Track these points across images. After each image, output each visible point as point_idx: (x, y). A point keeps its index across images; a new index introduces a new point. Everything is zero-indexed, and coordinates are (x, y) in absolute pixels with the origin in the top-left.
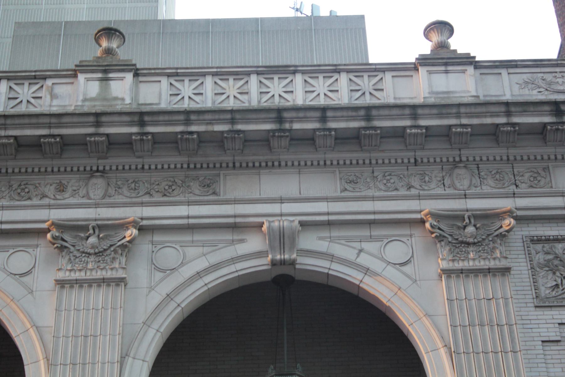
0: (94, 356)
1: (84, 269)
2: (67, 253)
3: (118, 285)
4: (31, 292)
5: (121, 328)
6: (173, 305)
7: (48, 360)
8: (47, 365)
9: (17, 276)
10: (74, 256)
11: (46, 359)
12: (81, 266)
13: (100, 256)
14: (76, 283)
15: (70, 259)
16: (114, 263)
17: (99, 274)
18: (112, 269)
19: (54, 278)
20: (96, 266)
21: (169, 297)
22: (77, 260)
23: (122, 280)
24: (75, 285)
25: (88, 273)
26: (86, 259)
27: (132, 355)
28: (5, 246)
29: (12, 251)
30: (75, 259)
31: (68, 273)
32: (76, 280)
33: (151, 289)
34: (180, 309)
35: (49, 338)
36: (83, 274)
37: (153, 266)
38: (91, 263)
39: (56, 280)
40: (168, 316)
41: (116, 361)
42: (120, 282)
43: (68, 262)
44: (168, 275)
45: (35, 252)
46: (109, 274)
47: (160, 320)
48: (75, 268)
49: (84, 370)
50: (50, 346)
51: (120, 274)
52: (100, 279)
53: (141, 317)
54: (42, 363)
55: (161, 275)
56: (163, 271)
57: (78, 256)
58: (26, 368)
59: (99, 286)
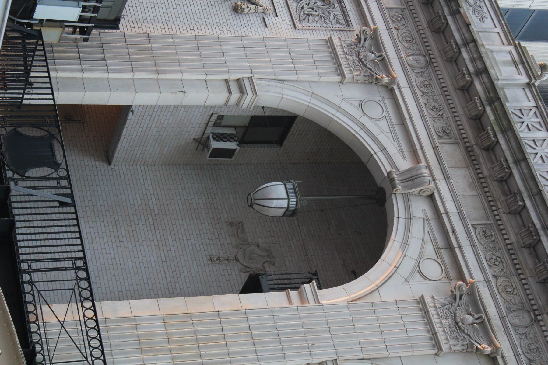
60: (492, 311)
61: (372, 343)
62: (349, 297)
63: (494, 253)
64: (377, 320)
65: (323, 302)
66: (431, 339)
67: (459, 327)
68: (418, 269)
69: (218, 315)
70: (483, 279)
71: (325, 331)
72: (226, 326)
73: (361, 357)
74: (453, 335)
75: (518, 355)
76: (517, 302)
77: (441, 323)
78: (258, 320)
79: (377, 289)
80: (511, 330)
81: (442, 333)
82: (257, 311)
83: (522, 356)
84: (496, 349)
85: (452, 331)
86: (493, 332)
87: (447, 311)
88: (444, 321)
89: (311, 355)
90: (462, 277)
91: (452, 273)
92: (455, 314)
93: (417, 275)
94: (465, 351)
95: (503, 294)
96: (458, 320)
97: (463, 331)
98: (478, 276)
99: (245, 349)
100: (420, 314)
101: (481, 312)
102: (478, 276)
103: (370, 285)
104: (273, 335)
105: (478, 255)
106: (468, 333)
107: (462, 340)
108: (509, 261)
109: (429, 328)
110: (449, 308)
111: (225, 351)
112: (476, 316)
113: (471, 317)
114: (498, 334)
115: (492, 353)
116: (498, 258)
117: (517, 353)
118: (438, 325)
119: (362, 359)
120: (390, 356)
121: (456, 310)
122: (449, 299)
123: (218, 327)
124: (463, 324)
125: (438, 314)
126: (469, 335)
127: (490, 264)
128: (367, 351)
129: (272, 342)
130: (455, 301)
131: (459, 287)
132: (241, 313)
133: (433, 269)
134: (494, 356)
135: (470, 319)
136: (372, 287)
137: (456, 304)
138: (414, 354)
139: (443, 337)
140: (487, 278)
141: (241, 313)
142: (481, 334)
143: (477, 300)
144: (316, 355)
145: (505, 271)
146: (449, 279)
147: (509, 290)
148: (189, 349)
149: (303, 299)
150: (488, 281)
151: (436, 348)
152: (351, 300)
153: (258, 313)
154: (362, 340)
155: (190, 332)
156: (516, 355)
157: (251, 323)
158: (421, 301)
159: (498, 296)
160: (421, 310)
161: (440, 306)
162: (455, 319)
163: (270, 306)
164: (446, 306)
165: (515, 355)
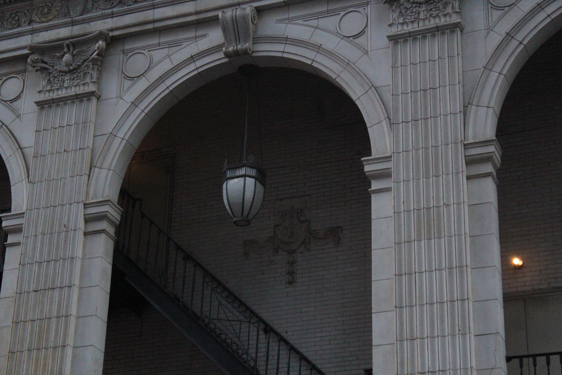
0: (435, 108)
1: (417, 20)
2: (396, 6)
3: (453, 32)
4: (367, 53)
5: (461, 77)
6: (514, 43)
7: (390, 119)
8: (389, 125)
9: (351, 38)
10: (405, 8)
11: (387, 119)
12: (413, 17)
13: (431, 3)
14: (410, 36)
15: (401, 12)
16: (447, 9)
17: (432, 23)
18: (445, 15)
19: (387, 35)
20: (428, 15)
21: (509, 36)
22: (409, 11)
23: (457, 25)
24: (409, 39)
25: (421, 24)
26: (417, 9)
27: (475, 103)
28: (336, 9)
29: (343, 13)
30: (406, 12)
31: (400, 27)
32: (409, 33)
33: (489, 29)
34: (523, 46)
35: (388, 97)
36: (416, 25)
37: (490, 5)
38: (423, 13)
39: (388, 37)
40: (510, 56)
41: (459, 111)
42: (454, 27)
43: (399, 15)
44: (506, 14)
45: (366, 11)
46: (442, 21)
47: (501, 61)
48: (407, 21)
49: (426, 126)
50: (390, 105)
51: (455, 19)
52: (434, 28)
53: (481, 62)
54: (385, 124)
55: (500, 13)
56: (501, 8)
57: (408, 7)
58: (369, 130)
59: (433, 36)
60: (64, 32)
61: (75, 163)
62: (24, 181)
63: (7, 19)
64: (52, 154)
65: (24, 208)
66: (81, 101)
67: (74, 69)
68: (9, 102)
69: (17, 323)
70: (30, 36)
71: (54, 212)
72: (30, 316)
73: (86, 177)
74: (82, 77)
75: (113, 14)
76: (60, 4)
77: (67, 88)
78: (29, 281)
79: (21, 149)
80: (86, 16)
81: (77, 88)
82: (20, 280)
83: (115, 10)
84: (101, 35)
85: (77, 77)
86: (85, 35)
87: (56, 79)
88: (65, 85)
89: (75, 230)
90: (24, 58)
91: (20, 67)
92: (60, 71)
93: (14, 104)
94: (100, 68)
95: (49, 18)
96: (66, 69)
97: (79, 66)
98: (26, 41)
99: (56, 299)
100: (54, 108)
101: (62, 45)
102: (26, 41)
103: (16, 156)
104: (47, 267)
105: (5, 36)
106: (82, 61)
107: (87, 69)
108: (17, 5)
109: (70, 101)
110: (54, 76)
111: (54, 320)
112: (65, 50)
113: (66, 55)
114: (88, 31)
115: (105, 40)
116: (12, 16)
117: (110, 15)
118: (69, 91)
119: (89, 176)
120: (91, 147)
121: (56, 69)
122: (44, 75)
123: (29, 325)
124: (72, 65)
125: (58, 89)
126: (85, 61)
127: (16, 26)
128: (81, 170)
129: (55, 269)
130: (48, 69)
131: (33, 62)
132: (19, 298)
133: (12, 87)
134: (109, 39)
135: (67, 57)
136: (19, 154)
137: (51, 69)
138: (94, 121)
139: (82, 88)
140: (30, 31)
141: (19, 298)
142: (85, 48)
143: (52, 45)
144: (76, 225)
145: (26, 11)
146: (25, 71)
147: (46, 10)
148: (45, 359)
149: (18, 230)
150: (33, 30)
151: (91, 98)
152: (27, 179)
153: (22, 281)
154: (69, 174)
155: (29, 357)
156: (112, 15)
157: (32, 289)
158: (41, 104)
159: (51, 23)
160: (50, 107)
161: (50, 86)
162: (66, 73)
163: (17, 266)
164: (52, 79)
165: (112, 18)
